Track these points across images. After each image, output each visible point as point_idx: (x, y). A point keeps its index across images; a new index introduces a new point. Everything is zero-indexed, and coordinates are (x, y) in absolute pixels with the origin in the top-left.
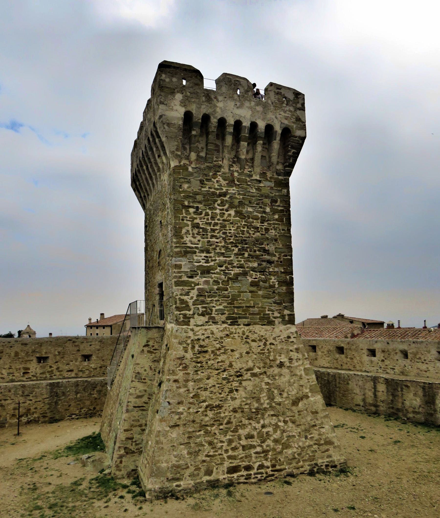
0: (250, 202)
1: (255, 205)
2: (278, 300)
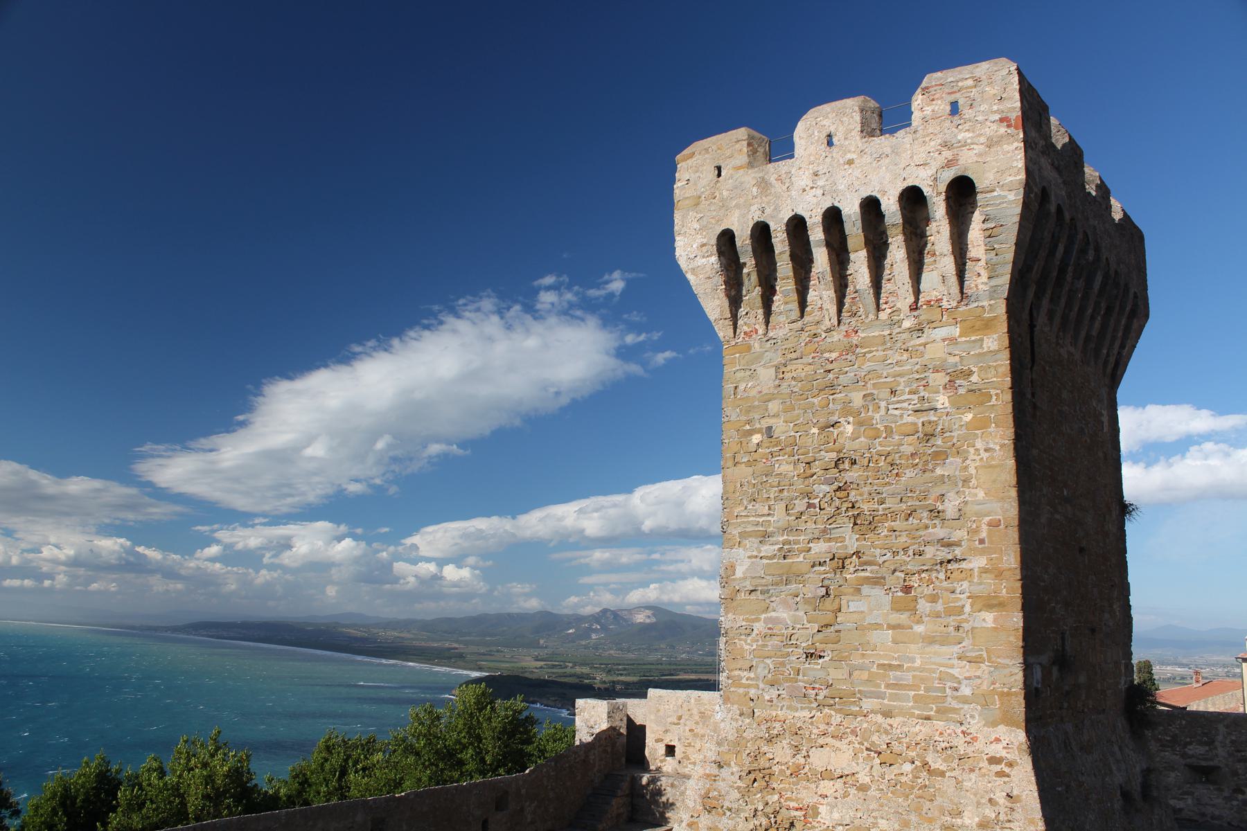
0: (893, 392)
1: (906, 397)
2: (972, 650)
